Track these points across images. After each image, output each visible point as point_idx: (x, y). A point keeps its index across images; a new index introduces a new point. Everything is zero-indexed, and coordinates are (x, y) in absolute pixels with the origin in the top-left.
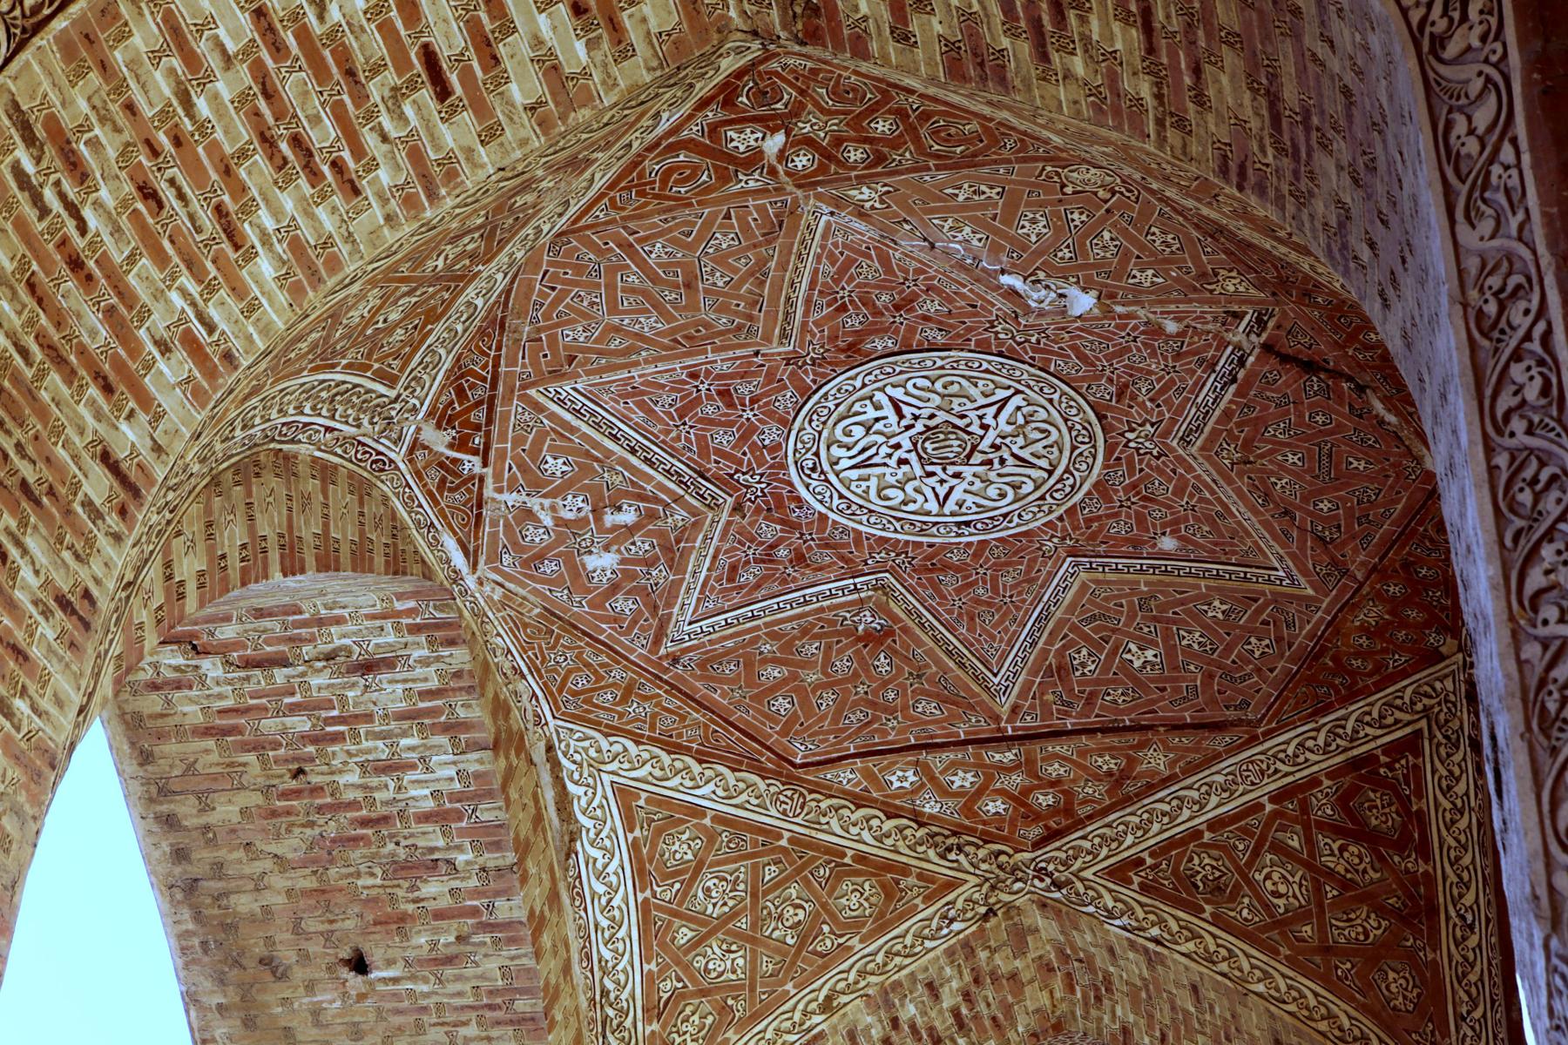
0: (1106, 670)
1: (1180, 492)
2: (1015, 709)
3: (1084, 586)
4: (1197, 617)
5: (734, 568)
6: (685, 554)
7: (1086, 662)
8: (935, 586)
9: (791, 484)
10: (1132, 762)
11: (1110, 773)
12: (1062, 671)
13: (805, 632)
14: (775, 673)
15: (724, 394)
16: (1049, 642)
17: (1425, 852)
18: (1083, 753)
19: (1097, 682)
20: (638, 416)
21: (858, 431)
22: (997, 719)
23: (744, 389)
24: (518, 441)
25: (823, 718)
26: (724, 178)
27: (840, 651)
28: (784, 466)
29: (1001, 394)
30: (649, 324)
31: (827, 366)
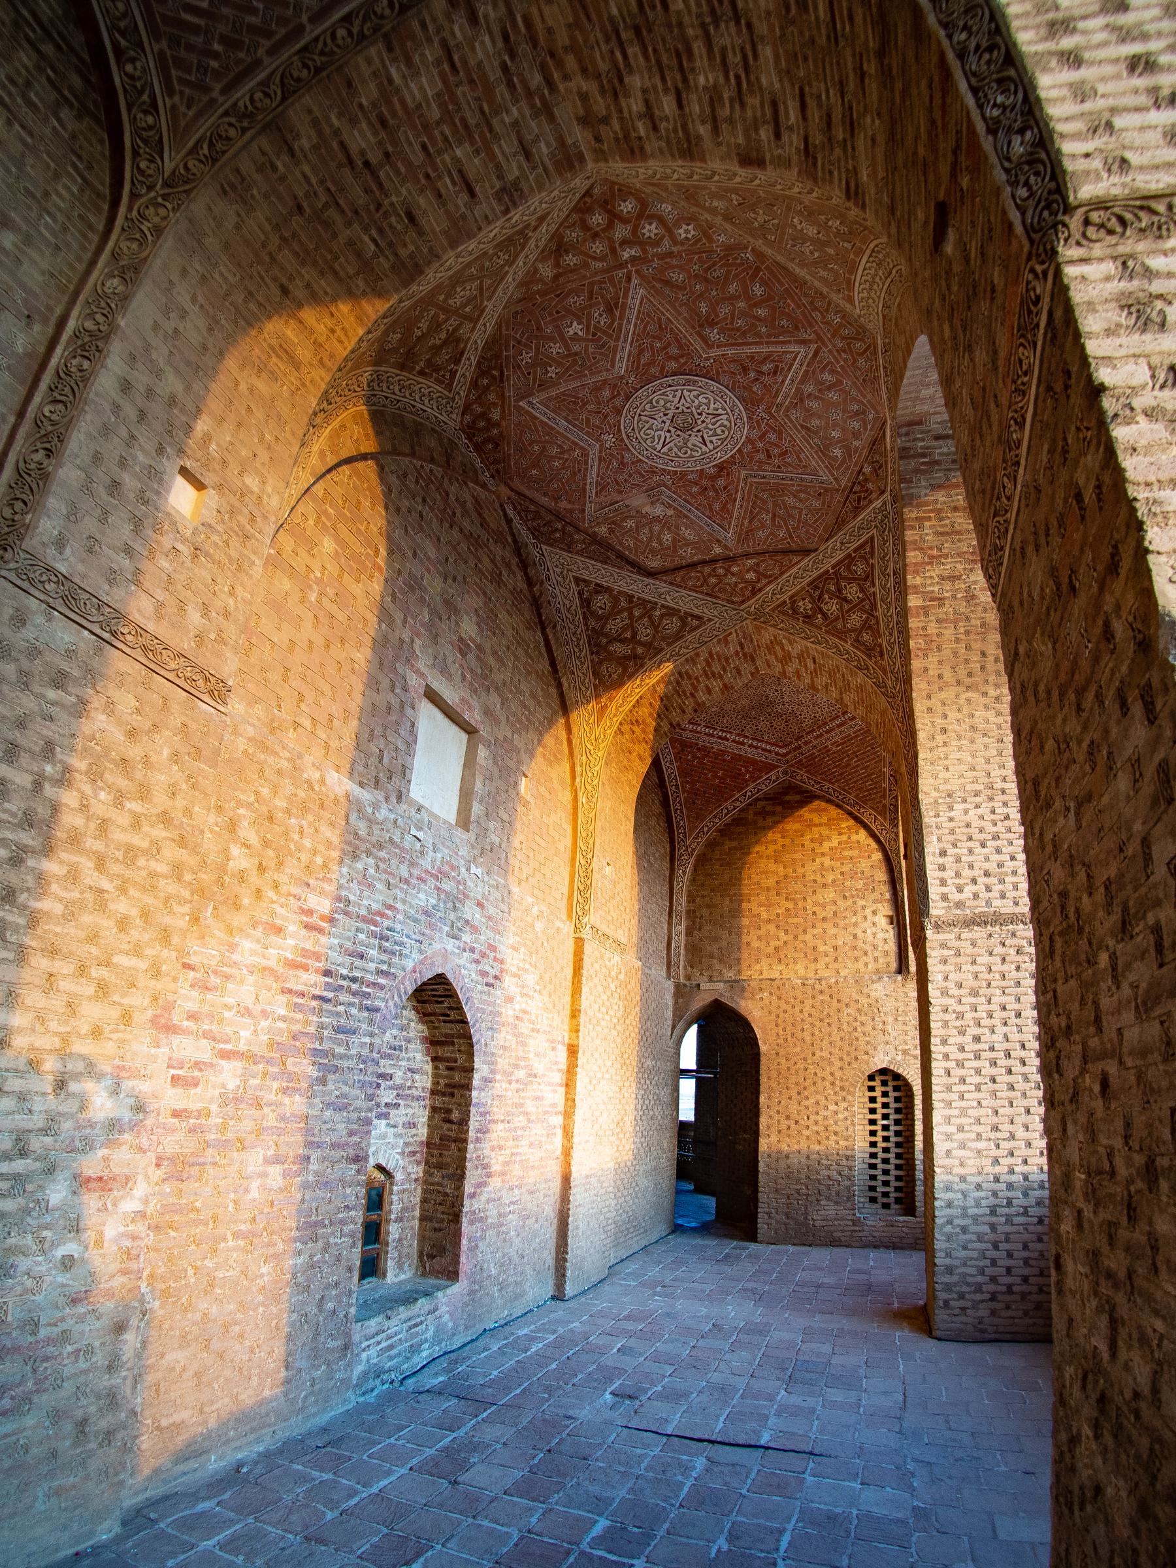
0: (589, 314)
1: (588, 420)
2: (629, 279)
3: (613, 365)
4: (560, 364)
5: (775, 373)
6: (795, 397)
7: (599, 317)
8: (680, 347)
9: (746, 409)
10: (557, 265)
11: (567, 252)
12: (610, 310)
13: (744, 334)
14: (761, 312)
15: (769, 456)
16: (620, 325)
17: (422, 373)
18: (585, 265)
19: (591, 306)
20: (802, 456)
21: (719, 431)
22: (637, 272)
23: (761, 456)
24: (848, 468)
25: (736, 275)
26: (758, 564)
27: (725, 319)
28: (750, 418)
29: (665, 450)
30: (790, 500)
31: (732, 461)
